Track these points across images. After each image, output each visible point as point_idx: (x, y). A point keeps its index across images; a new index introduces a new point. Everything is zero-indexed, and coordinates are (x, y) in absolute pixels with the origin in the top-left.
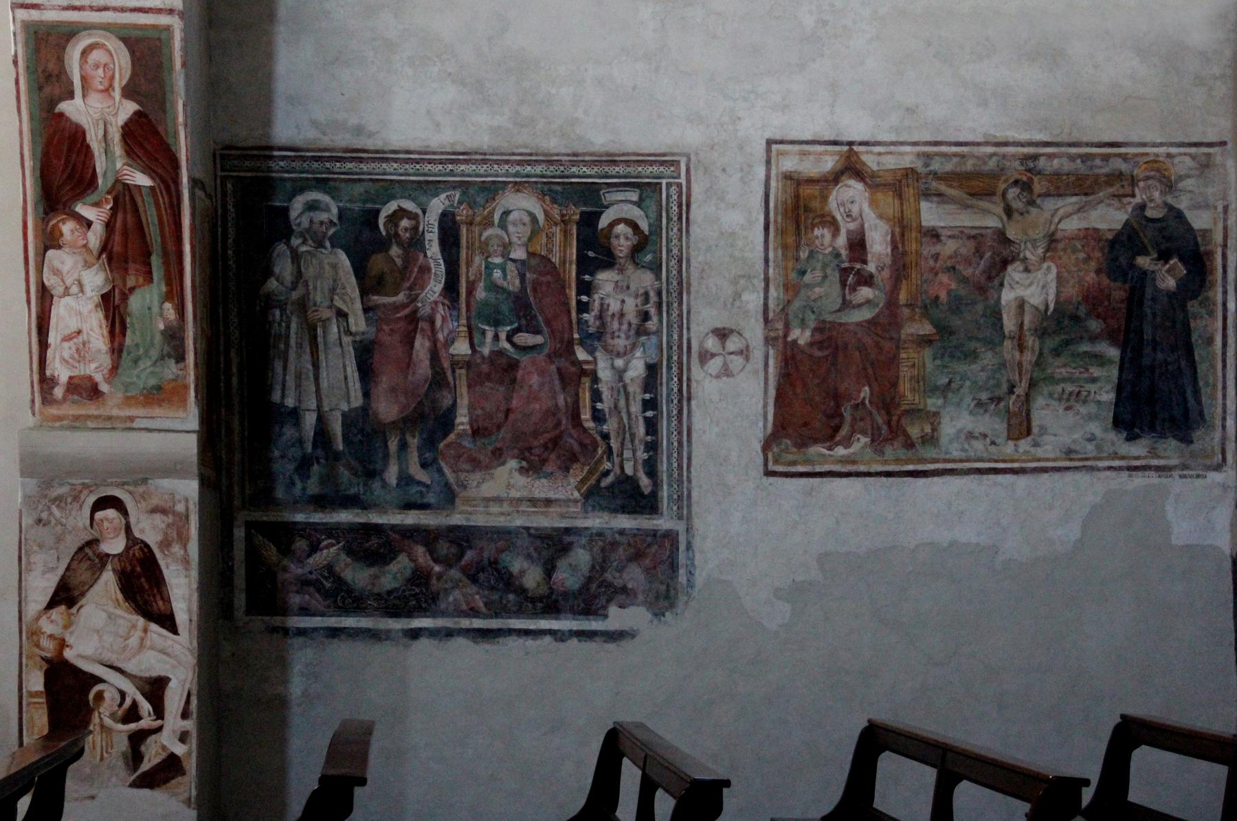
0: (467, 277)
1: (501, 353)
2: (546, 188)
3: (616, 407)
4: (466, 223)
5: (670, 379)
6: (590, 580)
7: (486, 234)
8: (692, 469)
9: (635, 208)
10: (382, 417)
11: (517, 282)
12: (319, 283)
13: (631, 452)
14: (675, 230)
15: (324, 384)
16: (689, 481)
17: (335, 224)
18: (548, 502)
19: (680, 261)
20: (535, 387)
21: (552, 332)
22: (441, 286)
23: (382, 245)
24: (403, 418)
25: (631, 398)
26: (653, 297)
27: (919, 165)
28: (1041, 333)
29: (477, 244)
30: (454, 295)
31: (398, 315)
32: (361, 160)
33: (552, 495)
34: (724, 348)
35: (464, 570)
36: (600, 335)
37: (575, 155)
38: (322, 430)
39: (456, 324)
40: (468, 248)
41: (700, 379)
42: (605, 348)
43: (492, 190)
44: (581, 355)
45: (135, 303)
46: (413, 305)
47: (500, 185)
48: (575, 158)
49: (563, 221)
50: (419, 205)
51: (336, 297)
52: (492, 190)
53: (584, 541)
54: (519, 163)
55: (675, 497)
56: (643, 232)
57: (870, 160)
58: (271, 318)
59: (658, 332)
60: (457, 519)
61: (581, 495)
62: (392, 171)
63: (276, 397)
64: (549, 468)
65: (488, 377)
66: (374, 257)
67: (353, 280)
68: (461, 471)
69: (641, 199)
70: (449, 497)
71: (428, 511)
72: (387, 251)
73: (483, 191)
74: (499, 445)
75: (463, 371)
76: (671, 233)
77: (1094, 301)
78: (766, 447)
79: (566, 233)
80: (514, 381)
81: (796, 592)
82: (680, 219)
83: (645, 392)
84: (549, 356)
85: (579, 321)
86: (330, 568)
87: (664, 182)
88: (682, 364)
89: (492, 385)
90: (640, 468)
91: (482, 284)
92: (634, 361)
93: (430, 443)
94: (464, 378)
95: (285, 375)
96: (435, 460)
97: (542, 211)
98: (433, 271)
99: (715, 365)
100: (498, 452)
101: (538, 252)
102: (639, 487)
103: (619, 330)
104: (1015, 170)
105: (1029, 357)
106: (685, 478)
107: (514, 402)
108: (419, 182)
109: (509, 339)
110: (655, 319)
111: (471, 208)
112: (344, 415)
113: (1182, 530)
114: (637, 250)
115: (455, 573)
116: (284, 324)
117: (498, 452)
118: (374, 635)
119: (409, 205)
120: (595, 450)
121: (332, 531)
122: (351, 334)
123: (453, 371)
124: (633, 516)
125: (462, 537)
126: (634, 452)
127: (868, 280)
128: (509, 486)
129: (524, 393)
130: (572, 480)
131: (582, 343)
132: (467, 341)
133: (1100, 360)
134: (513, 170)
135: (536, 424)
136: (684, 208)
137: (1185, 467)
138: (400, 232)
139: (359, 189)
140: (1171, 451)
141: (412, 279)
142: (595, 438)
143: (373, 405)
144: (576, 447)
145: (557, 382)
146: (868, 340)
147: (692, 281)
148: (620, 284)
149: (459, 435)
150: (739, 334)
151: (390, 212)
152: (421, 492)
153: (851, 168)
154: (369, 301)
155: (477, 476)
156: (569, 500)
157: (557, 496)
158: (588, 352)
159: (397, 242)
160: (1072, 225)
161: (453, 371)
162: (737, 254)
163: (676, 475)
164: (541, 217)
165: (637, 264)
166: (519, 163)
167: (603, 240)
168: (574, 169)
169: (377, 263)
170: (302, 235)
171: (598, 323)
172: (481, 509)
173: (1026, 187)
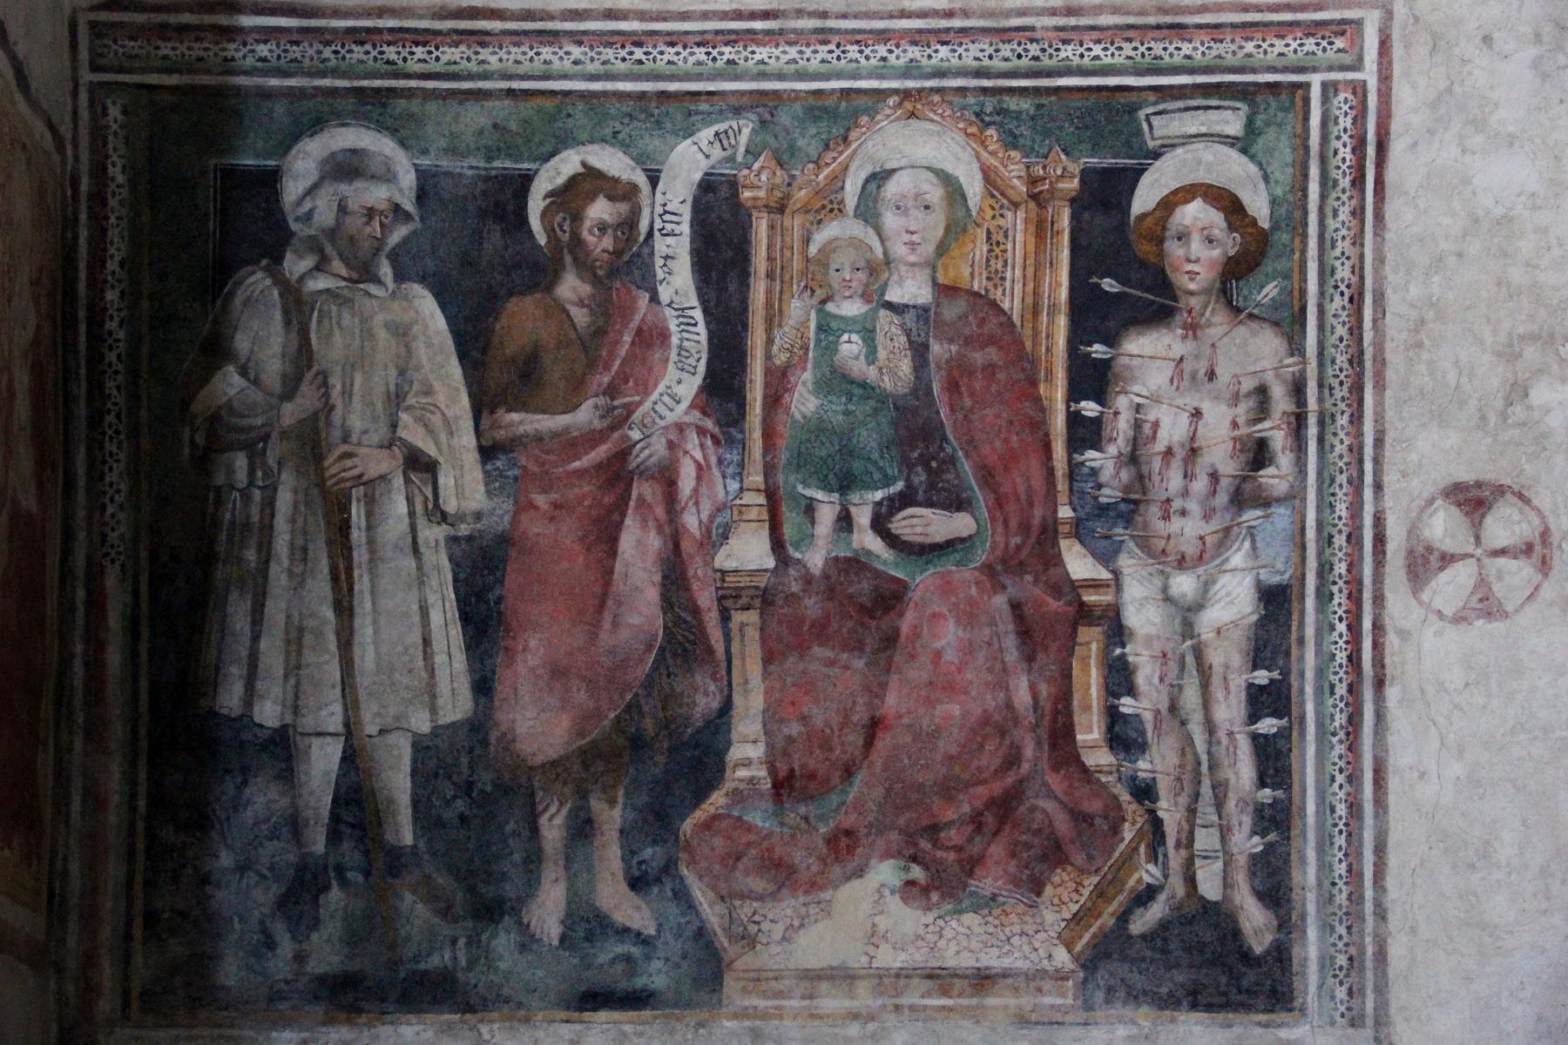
0: (768, 356)
1: (855, 564)
2: (990, 104)
3: (1173, 708)
4: (769, 209)
5: (1325, 628)
7: (820, 238)
8: (1390, 882)
9: (1234, 154)
10: (524, 747)
11: (906, 366)
12: (358, 378)
13: (1215, 832)
14: (1344, 213)
15: (366, 656)
16: (1381, 914)
17: (408, 217)
18: (983, 980)
19: (1356, 300)
20: (951, 656)
21: (999, 503)
22: (697, 381)
24: (582, 751)
25: (1216, 681)
26: (1281, 403)
29: (797, 263)
30: (732, 406)
31: (577, 464)
32: (481, 38)
33: (992, 960)
34: (1478, 539)
36: (1129, 509)
37: (1070, 11)
38: (357, 788)
39: (734, 486)
40: (770, 276)
41: (1406, 624)
42: (1144, 544)
44: (1079, 564)
46: (616, 435)
47: (862, 101)
48: (1073, 21)
49: (1034, 197)
50: (640, 159)
51: (405, 417)
54: (917, 38)
55: (1342, 960)
56: (1254, 222)
58: (220, 479)
59: (1295, 496)
61: (1076, 958)
63: (230, 699)
64: (986, 883)
65: (820, 631)
66: (513, 305)
67: (455, 370)
68: (743, 897)
69: (1251, 129)
71: (646, 1013)
72: (549, 287)
73: (816, 119)
74: (849, 821)
75: (753, 617)
76: (1331, 224)
79: (1041, 230)
80: (890, 640)
82: (1358, 181)
83: (1255, 667)
84: (988, 569)
85: (1073, 471)
87: (1316, 80)
88: (1360, 583)
89: (829, 654)
90: (1241, 878)
91: (807, 376)
92: (1225, 579)
94: (753, 634)
95: (256, 637)
96: (669, 867)
97: (976, 165)
98: (675, 340)
99: (1452, 586)
100: (844, 842)
101: (965, 284)
102: (1237, 933)
103: (1185, 493)
106: (1369, 907)
107: (892, 701)
108: (642, 96)
109: (879, 525)
110: (1285, 461)
111: (781, 166)
112: (422, 748)
116: (257, 494)
117: (844, 842)
119: (612, 162)
120: (1115, 831)
122: (444, 517)
123: (725, 617)
124: (1221, 1017)
126: (1225, 833)
128: (874, 937)
129: (918, 673)
130: (1049, 916)
131: (1079, 530)
132: (765, 533)
134: (898, 59)
135: (950, 758)
136: (1371, 151)
138: (585, 235)
139: (475, 117)
141: (617, 363)
142: (1115, 798)
143: (501, 716)
144: (1062, 824)
145: (1010, 642)
147: (1389, 355)
148: (1187, 367)
149: (737, 796)
150: (1521, 496)
151: (560, 181)
152: (628, 959)
154: (496, 425)
155: (788, 907)
156: (1042, 974)
157: (1007, 962)
158: (1094, 554)
159: (575, 259)
161: (725, 617)
162: (1517, 276)
163: (1342, 899)
164: (974, 188)
165: (1238, 310)
166: (917, 38)
167: (1144, 248)
168: (1067, 51)
170: (314, 245)
171: (1125, 475)
172: (795, 1003)
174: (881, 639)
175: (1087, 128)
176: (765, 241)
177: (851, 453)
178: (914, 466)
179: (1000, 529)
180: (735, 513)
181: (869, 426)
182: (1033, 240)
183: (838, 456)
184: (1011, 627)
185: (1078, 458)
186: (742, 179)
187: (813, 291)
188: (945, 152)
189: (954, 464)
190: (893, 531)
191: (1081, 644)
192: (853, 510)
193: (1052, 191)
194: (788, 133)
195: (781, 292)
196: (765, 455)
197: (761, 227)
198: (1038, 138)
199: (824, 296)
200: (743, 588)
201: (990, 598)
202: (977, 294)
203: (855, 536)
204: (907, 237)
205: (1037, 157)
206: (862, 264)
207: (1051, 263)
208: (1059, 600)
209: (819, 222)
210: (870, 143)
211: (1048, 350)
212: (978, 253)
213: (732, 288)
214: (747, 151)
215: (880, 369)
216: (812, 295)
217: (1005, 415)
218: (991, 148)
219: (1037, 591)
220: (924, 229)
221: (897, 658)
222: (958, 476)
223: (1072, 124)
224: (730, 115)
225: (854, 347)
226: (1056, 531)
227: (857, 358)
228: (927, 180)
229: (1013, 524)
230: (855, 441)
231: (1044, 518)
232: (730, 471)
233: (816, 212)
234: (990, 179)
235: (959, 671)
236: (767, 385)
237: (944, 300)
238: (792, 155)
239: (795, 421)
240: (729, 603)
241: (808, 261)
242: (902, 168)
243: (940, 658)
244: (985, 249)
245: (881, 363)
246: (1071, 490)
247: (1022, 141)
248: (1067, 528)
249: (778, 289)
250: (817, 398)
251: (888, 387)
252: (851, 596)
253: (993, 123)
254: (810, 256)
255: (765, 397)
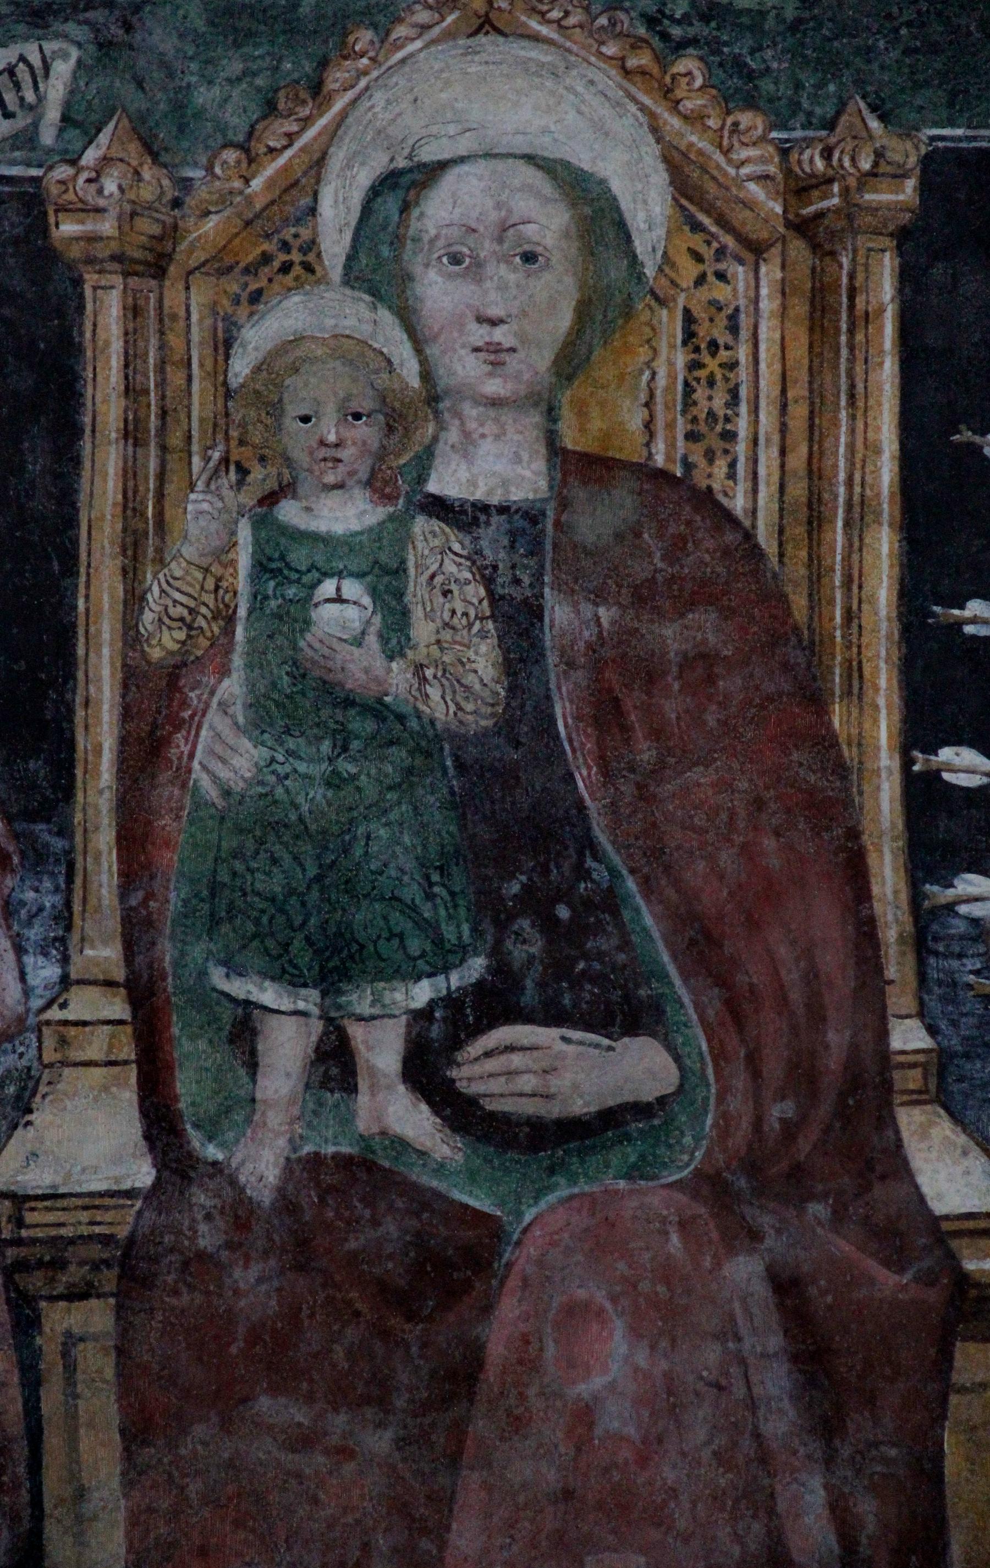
89: (301, 1415)
101: (632, 452)
132: (129, 1096)
174: (433, 1373)
175: (934, 49)
176: (117, 346)
177: (349, 886)
178: (512, 917)
179: (740, 1081)
180: (49, 1042)
181: (394, 816)
182: (804, 339)
183: (315, 894)
184: (775, 1342)
185: (938, 894)
186: (54, 190)
187: (243, 471)
188: (571, 116)
189: (615, 912)
190: (462, 1086)
191: (962, 1390)
192: (356, 1032)
193: (850, 210)
194: (171, 75)
195: (161, 477)
196: (124, 890)
198: (809, 81)
199: (272, 484)
200: (72, 1241)
201: (718, 1265)
202: (662, 475)
203: (363, 1099)
204: (479, 334)
205: (807, 125)
206: (366, 405)
207: (852, 397)
208: (901, 1270)
209: (256, 297)
210: (379, 97)
211: (849, 616)
212: (662, 372)
213: (36, 465)
214: (66, 119)
215: (419, 668)
216: (240, 483)
217: (743, 785)
218: (688, 105)
219: (843, 1247)
220: (525, 314)
221: (480, 1426)
222: (625, 944)
223: (895, 39)
224: (21, 28)
225: (351, 612)
226: (887, 1087)
227: (358, 641)
228: (527, 188)
229: (774, 1069)
230: (358, 852)
231: (854, 1048)
232: (34, 933)
233: (246, 271)
235: (643, 1461)
236: (127, 714)
237: (579, 493)
238: (182, 129)
239: (200, 803)
240: (35, 1282)
241: (228, 395)
242: (462, 160)
243: (591, 1425)
244: (681, 359)
245: (419, 655)
246: (922, 977)
247: (767, 86)
248: (913, 1080)
249: (153, 465)
250: (258, 743)
251: (440, 714)
252: (353, 1258)
253: (693, 42)
254: (234, 383)
255: (123, 741)
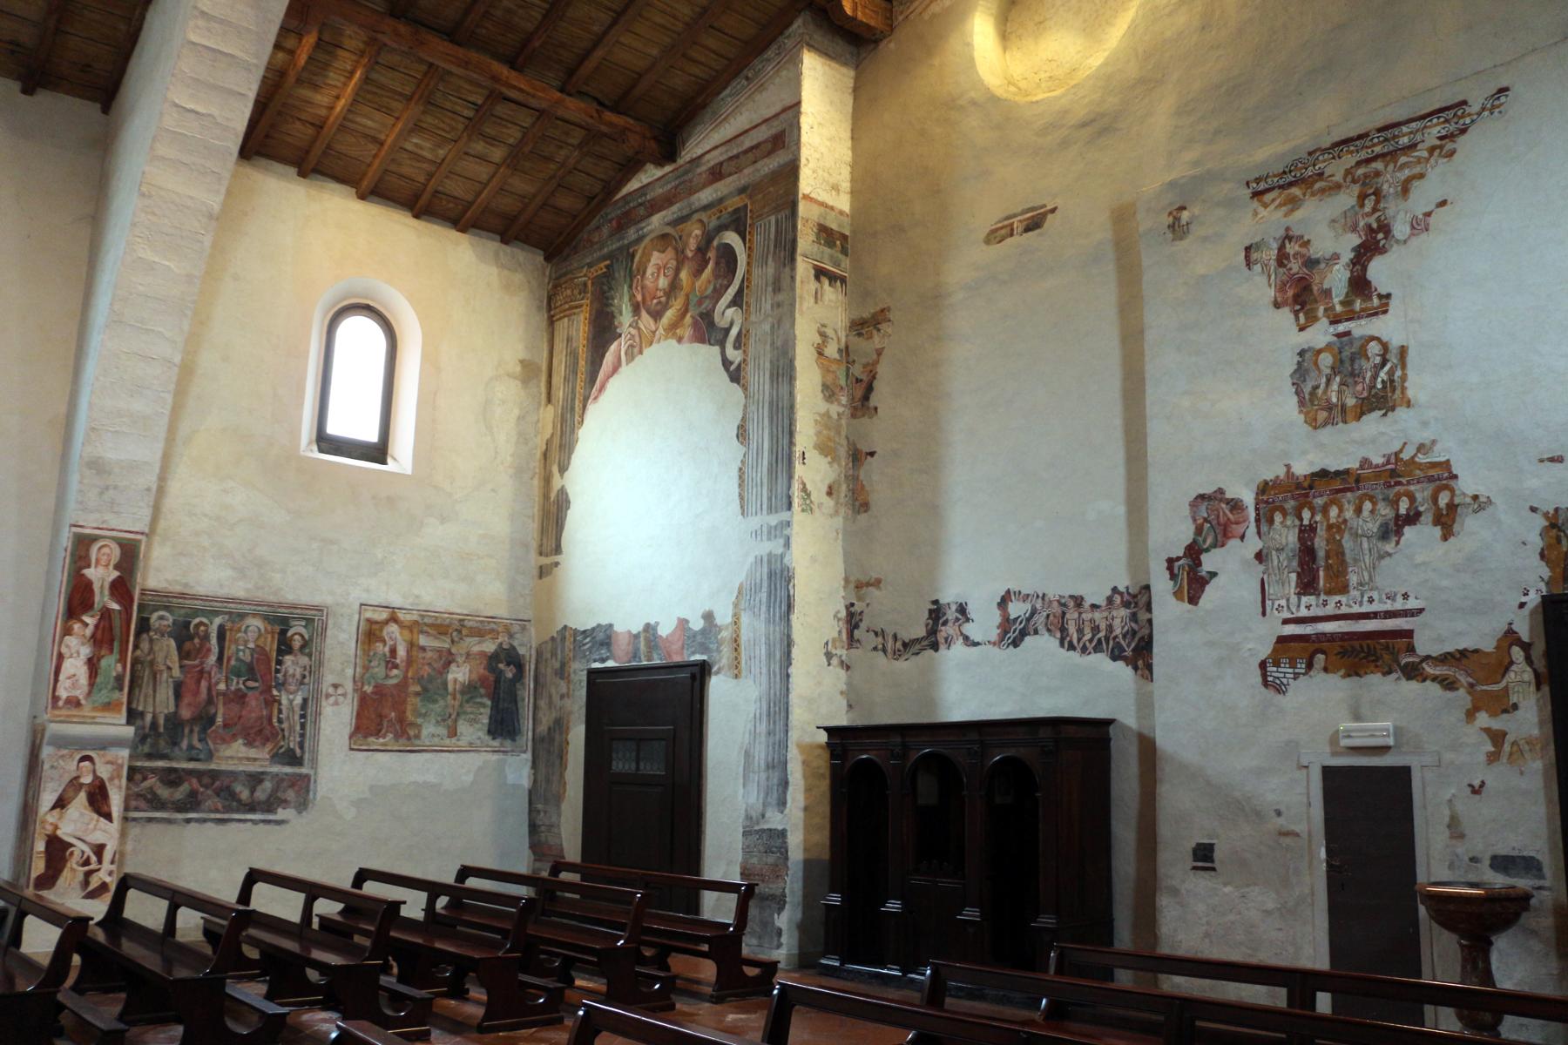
1: (239, 690)
6: (271, 796)
15: (158, 699)
23: (191, 638)
26: (308, 667)
27: (419, 619)
28: (463, 693)
35: (214, 791)
36: (283, 684)
42: (286, 690)
43: (242, 616)
44: (275, 692)
45: (104, 663)
52: (242, 616)
53: (269, 777)
57: (401, 615)
59: (309, 684)
60: (213, 766)
62: (198, 604)
64: (257, 743)
65: (233, 700)
70: (210, 756)
77: (483, 681)
78: (350, 738)
79: (273, 637)
80: (244, 703)
81: (358, 803)
86: (151, 788)
93: (204, 730)
99: (332, 700)
104: (456, 625)
105: (457, 703)
109: (244, 683)
112: (166, 716)
113: (511, 778)
114: (303, 647)
115: (209, 792)
118: (169, 821)
119: (205, 620)
121: (153, 771)
125: (214, 775)
127: (396, 666)
129: (248, 709)
131: (275, 687)
133: (484, 705)
137: (513, 751)
139: (183, 611)
140: (508, 744)
146: (395, 692)
153: (393, 619)
155: (224, 746)
160: (476, 649)
164: (263, 630)
169: (187, 645)
173: (460, 632)
197: (228, 633)
234: (266, 629)
